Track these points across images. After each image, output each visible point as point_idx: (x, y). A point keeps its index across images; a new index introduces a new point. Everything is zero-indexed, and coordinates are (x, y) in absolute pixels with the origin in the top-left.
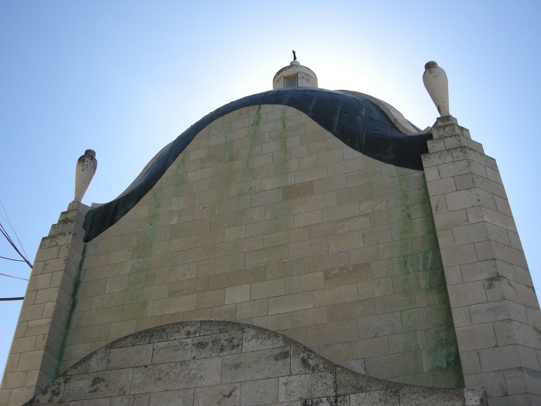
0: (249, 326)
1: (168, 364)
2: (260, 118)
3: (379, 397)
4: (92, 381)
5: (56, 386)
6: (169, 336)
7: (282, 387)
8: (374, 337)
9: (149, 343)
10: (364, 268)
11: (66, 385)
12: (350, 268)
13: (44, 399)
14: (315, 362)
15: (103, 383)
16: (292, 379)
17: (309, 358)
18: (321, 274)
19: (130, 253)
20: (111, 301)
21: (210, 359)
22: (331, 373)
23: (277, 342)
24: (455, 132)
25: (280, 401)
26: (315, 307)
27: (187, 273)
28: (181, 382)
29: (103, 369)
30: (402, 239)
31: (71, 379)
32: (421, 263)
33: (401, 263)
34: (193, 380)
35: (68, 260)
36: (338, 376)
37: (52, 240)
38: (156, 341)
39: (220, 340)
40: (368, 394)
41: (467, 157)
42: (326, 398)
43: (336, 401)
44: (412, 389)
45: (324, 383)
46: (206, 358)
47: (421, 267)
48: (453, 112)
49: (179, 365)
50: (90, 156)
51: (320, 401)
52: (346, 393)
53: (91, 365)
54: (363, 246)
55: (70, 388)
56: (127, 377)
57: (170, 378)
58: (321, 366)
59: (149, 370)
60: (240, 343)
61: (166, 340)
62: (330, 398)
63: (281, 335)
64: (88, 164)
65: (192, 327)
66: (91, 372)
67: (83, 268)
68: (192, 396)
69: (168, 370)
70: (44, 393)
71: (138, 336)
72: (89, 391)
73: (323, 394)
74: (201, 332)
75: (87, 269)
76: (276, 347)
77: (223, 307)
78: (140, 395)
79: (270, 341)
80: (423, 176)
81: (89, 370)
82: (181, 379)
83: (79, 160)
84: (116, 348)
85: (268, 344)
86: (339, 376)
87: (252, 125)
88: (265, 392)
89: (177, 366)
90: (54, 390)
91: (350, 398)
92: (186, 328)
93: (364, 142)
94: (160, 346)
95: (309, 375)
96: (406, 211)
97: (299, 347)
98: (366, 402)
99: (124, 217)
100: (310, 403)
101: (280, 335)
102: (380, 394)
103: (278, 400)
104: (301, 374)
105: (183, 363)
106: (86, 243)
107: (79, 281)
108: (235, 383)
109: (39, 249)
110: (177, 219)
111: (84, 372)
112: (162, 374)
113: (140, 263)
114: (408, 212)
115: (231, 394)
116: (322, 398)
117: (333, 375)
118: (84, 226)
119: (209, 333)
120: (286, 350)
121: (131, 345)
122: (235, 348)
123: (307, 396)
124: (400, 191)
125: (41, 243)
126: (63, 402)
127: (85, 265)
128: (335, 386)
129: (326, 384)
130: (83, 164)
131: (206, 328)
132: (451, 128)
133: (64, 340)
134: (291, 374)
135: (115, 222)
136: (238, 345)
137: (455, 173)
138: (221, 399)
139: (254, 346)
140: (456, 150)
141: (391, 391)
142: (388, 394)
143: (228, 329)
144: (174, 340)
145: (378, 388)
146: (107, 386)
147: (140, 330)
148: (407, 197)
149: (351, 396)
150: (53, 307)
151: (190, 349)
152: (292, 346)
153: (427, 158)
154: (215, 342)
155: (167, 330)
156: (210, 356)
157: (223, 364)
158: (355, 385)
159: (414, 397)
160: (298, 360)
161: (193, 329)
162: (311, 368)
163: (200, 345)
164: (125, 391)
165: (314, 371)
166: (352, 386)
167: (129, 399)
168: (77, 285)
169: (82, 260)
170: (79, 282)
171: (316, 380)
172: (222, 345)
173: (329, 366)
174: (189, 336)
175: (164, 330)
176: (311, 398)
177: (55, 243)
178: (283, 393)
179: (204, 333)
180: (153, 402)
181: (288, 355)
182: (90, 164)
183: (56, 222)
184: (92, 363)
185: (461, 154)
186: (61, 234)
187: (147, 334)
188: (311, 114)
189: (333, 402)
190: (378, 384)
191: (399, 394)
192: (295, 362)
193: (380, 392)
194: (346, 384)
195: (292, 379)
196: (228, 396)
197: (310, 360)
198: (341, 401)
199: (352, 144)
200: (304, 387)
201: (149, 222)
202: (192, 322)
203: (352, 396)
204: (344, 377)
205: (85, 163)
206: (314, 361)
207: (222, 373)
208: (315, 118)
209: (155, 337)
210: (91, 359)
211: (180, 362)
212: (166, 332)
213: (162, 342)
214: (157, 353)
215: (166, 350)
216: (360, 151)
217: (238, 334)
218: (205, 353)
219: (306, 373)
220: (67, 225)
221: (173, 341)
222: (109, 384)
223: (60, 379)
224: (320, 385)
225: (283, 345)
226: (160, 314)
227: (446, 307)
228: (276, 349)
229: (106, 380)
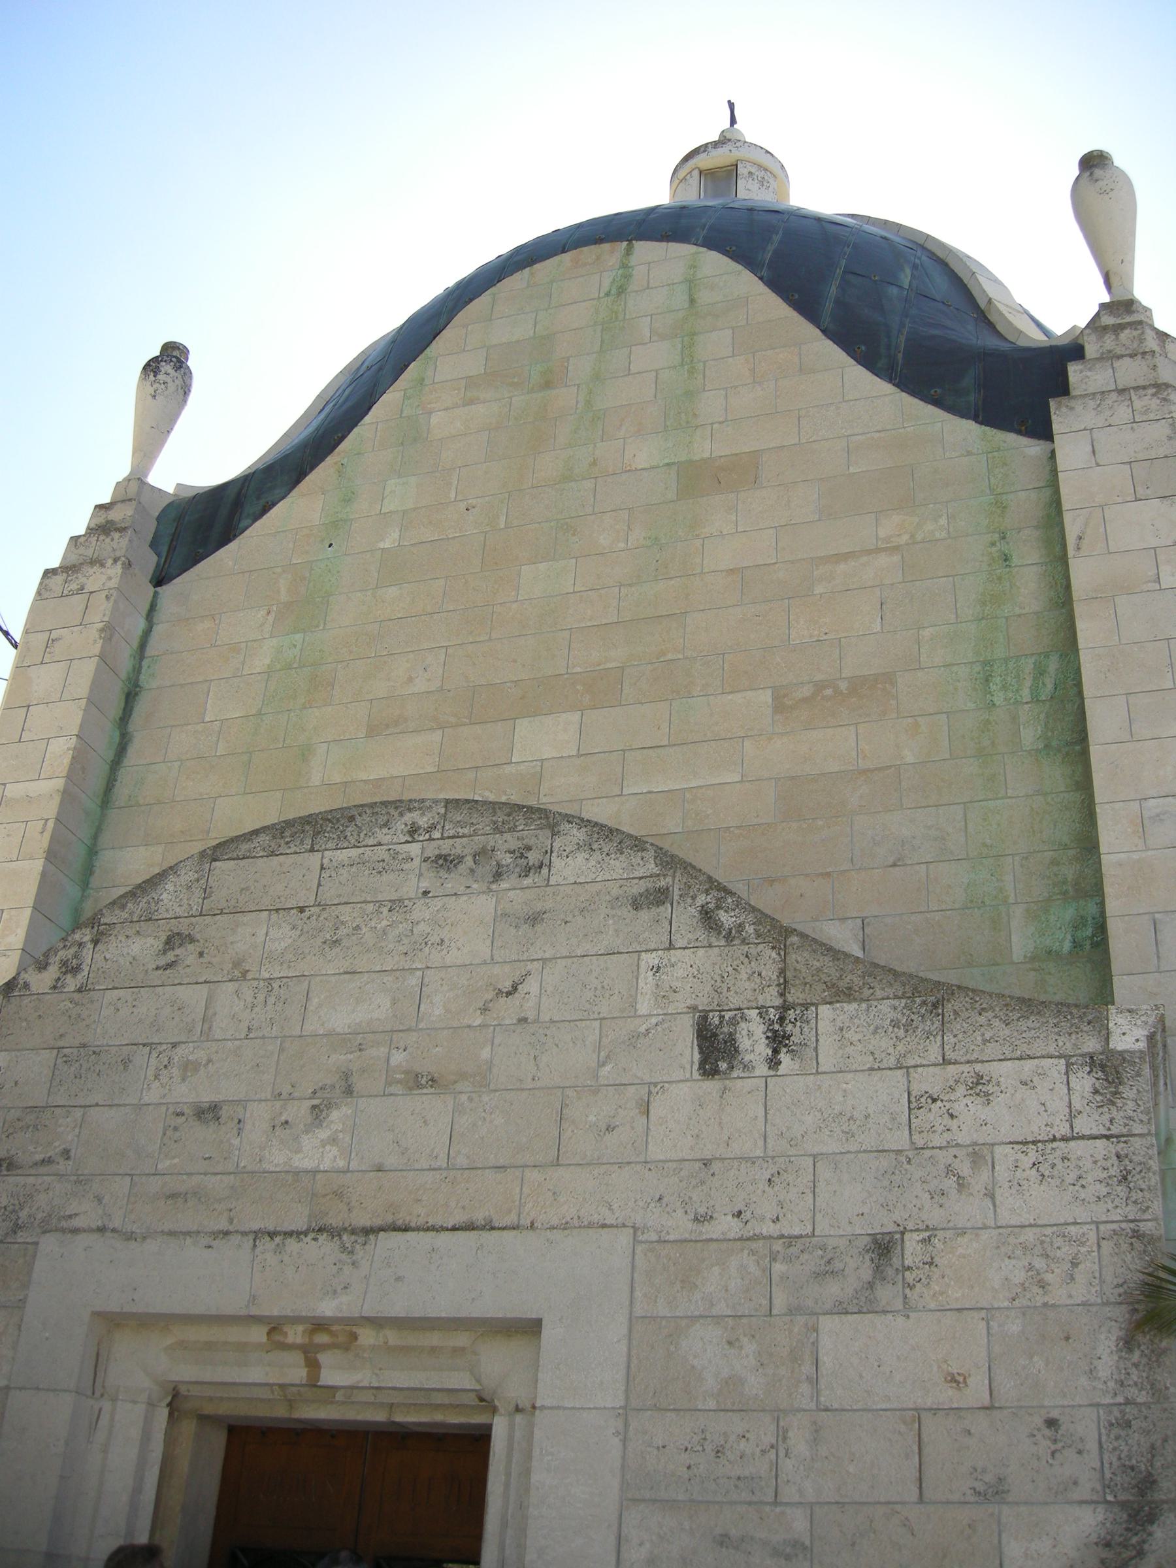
0: (569, 819)
1: (359, 905)
2: (628, 277)
3: (893, 1015)
4: (163, 940)
5: (72, 951)
6: (362, 835)
7: (646, 978)
8: (891, 866)
9: (312, 850)
10: (880, 686)
11: (96, 949)
12: (843, 686)
13: (41, 981)
14: (734, 919)
15: (190, 947)
16: (673, 960)
17: (719, 907)
18: (766, 697)
19: (271, 618)
20: (218, 740)
21: (465, 898)
22: (773, 948)
23: (641, 862)
24: (1144, 345)
25: (639, 1013)
26: (745, 779)
27: (417, 677)
28: (390, 953)
29: (194, 912)
30: (983, 618)
31: (111, 935)
32: (1028, 683)
33: (976, 679)
34: (421, 950)
35: (109, 631)
36: (792, 957)
37: (69, 578)
38: (330, 845)
39: (493, 851)
40: (864, 1005)
41: (1171, 412)
42: (758, 1011)
43: (782, 1019)
44: (978, 999)
45: (755, 972)
46: (456, 894)
47: (1026, 694)
48: (1143, 291)
49: (385, 910)
50: (173, 359)
51: (742, 1018)
52: (809, 1001)
53: (162, 900)
54: (879, 629)
55: (107, 957)
56: (253, 935)
57: (363, 940)
58: (750, 929)
59: (309, 918)
60: (546, 861)
61: (356, 844)
62: (767, 1011)
63: (652, 845)
64: (169, 380)
65: (423, 814)
66: (160, 917)
67: (149, 652)
68: (416, 989)
69: (358, 921)
70: (42, 966)
71: (283, 833)
72: (154, 967)
73: (750, 1001)
74: (447, 828)
75: (158, 656)
76: (637, 874)
77: (508, 769)
78: (285, 980)
79: (622, 858)
80: (1050, 455)
81: (156, 913)
82: (391, 946)
83: (144, 368)
84: (228, 859)
85: (618, 866)
86: (794, 956)
87: (608, 294)
88: (603, 987)
89: (382, 913)
90: (68, 960)
91: (817, 1014)
92: (409, 817)
93: (900, 356)
94: (340, 859)
95: (716, 950)
96: (998, 544)
97: (696, 879)
98: (858, 1027)
99: (258, 524)
100: (716, 1021)
101: (648, 846)
102: (895, 1009)
103: (636, 1010)
104: (697, 947)
105: (396, 905)
106: (159, 589)
107: (136, 685)
108: (529, 961)
109: (35, 600)
110: (396, 535)
111: (142, 918)
112: (343, 931)
113: (295, 646)
114: (1003, 549)
115: (515, 988)
116: (746, 1011)
117: (779, 954)
118: (154, 545)
119: (466, 831)
120: (663, 883)
121: (265, 854)
122: (532, 871)
123: (709, 1004)
124: (988, 491)
125: (41, 583)
126: (90, 989)
128: (782, 981)
129: (760, 975)
130: (154, 379)
131: (458, 819)
132: (1136, 333)
133: (95, 837)
134: (671, 947)
135: (235, 537)
136: (540, 867)
137: (1135, 452)
138: (491, 1001)
139: (580, 869)
140: (1141, 392)
141: (924, 1003)
142: (914, 1010)
143: (517, 824)
144: (375, 846)
145: (890, 992)
146: (201, 954)
147: (290, 816)
148: (1004, 507)
149: (821, 1008)
150: (69, 749)
151: (417, 871)
152: (678, 874)
153: (1064, 409)
154: (481, 854)
155: (358, 819)
156: (468, 891)
157: (499, 913)
158: (834, 981)
159: (982, 1020)
160: (693, 911)
161: (425, 819)
162: (724, 933)
163: (441, 862)
164: (247, 969)
165: (732, 941)
166: (825, 983)
167: (256, 991)
168: (131, 696)
169: (147, 633)
170: (138, 689)
171: (735, 963)
172: (498, 865)
173: (769, 931)
174: (416, 836)
175: (352, 819)
176: (718, 1008)
177: (78, 584)
178: (649, 992)
179: (453, 831)
180: (315, 1001)
181: (667, 898)
182: (174, 381)
183: (81, 531)
184: (164, 896)
185: (1155, 402)
186: (92, 562)
187: (307, 827)
188: (764, 273)
189: (773, 1021)
190: (892, 982)
191: (943, 1011)
192: (685, 916)
193: (896, 1002)
194: (810, 978)
195: (673, 960)
196: (509, 994)
197: (722, 912)
198: (795, 1019)
199: (868, 361)
200: (704, 980)
201: (323, 540)
202: (423, 801)
203: (824, 1010)
204: (807, 960)
205: (161, 377)
206: (731, 917)
207: (496, 934)
208: (777, 284)
209: (326, 835)
210: (162, 886)
211: (390, 901)
212: (356, 825)
213: (344, 848)
214: (330, 877)
215: (354, 869)
216: (890, 381)
217: (544, 836)
218: (454, 881)
219: (710, 946)
220: (108, 540)
221: (372, 848)
222: (206, 951)
223: (83, 934)
224: (745, 977)
225: (656, 870)
226: (345, 780)
227: (1084, 799)
228: (636, 881)
229: (198, 941)
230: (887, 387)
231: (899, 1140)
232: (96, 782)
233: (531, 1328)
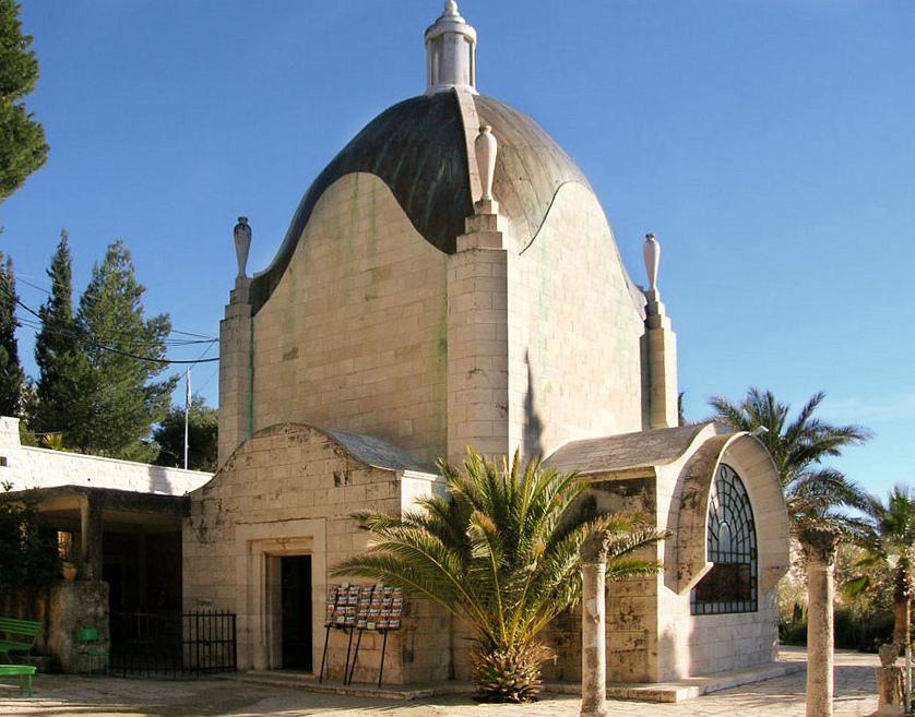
18: (393, 352)
105: (285, 448)
127: (255, 338)
154: (299, 436)
168: (252, 357)
208: (396, 193)
217: (307, 432)
230: (422, 238)
231: (364, 499)
232: (247, 388)
233: (312, 538)
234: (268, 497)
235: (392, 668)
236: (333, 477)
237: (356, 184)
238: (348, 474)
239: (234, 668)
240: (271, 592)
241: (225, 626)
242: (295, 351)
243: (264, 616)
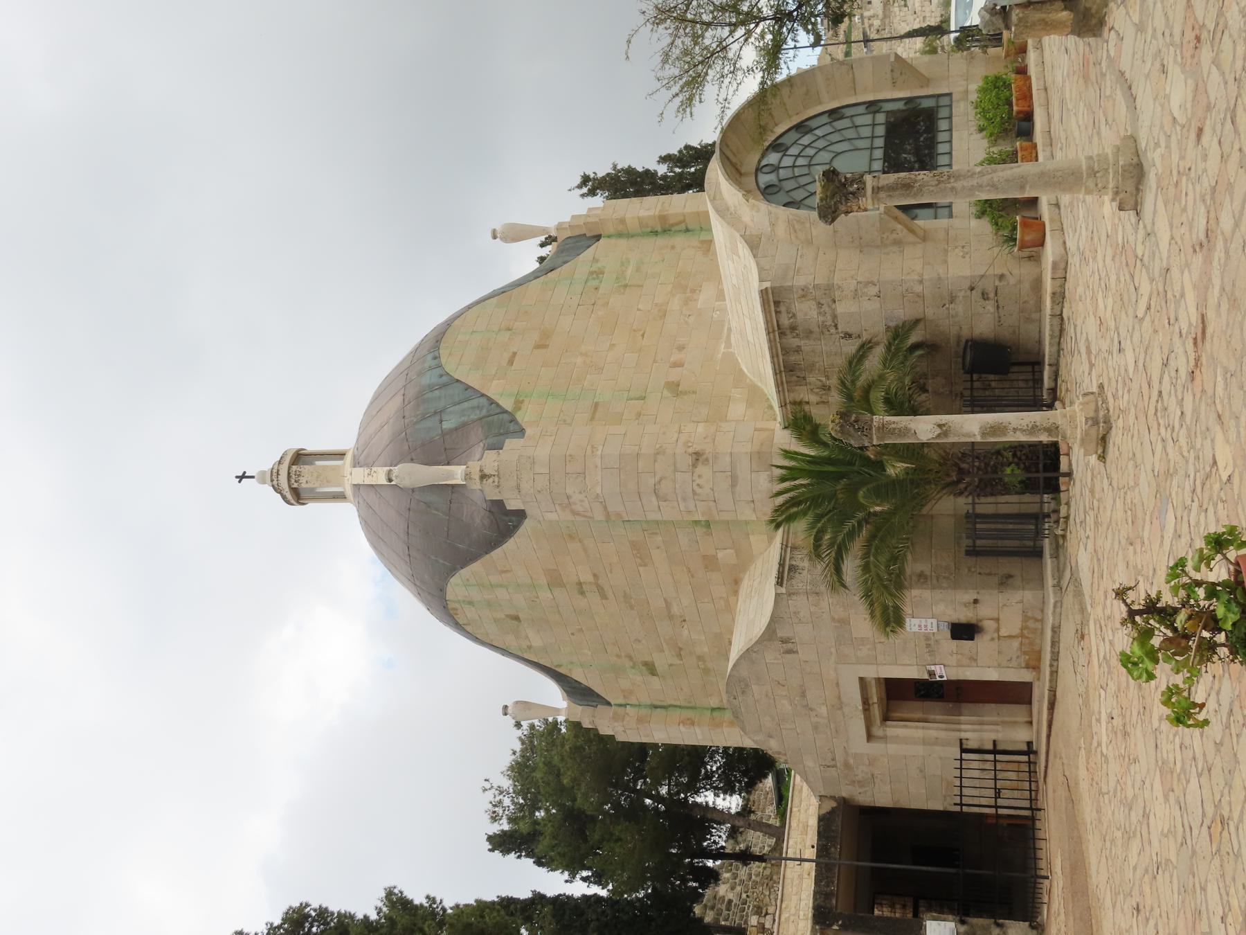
2: (464, 601)
12: (635, 552)
18: (641, 569)
133: (707, 709)
168: (656, 707)
233: (862, 679)
234: (815, 720)
235: (1022, 602)
236: (787, 655)
237: (459, 602)
238: (784, 641)
239: (1030, 750)
240: (932, 717)
241: (975, 765)
242: (646, 664)
243: (963, 727)
